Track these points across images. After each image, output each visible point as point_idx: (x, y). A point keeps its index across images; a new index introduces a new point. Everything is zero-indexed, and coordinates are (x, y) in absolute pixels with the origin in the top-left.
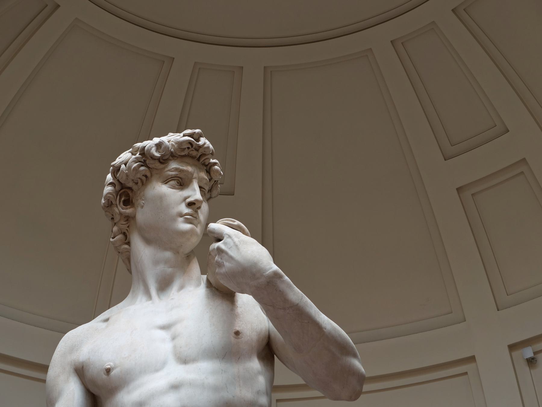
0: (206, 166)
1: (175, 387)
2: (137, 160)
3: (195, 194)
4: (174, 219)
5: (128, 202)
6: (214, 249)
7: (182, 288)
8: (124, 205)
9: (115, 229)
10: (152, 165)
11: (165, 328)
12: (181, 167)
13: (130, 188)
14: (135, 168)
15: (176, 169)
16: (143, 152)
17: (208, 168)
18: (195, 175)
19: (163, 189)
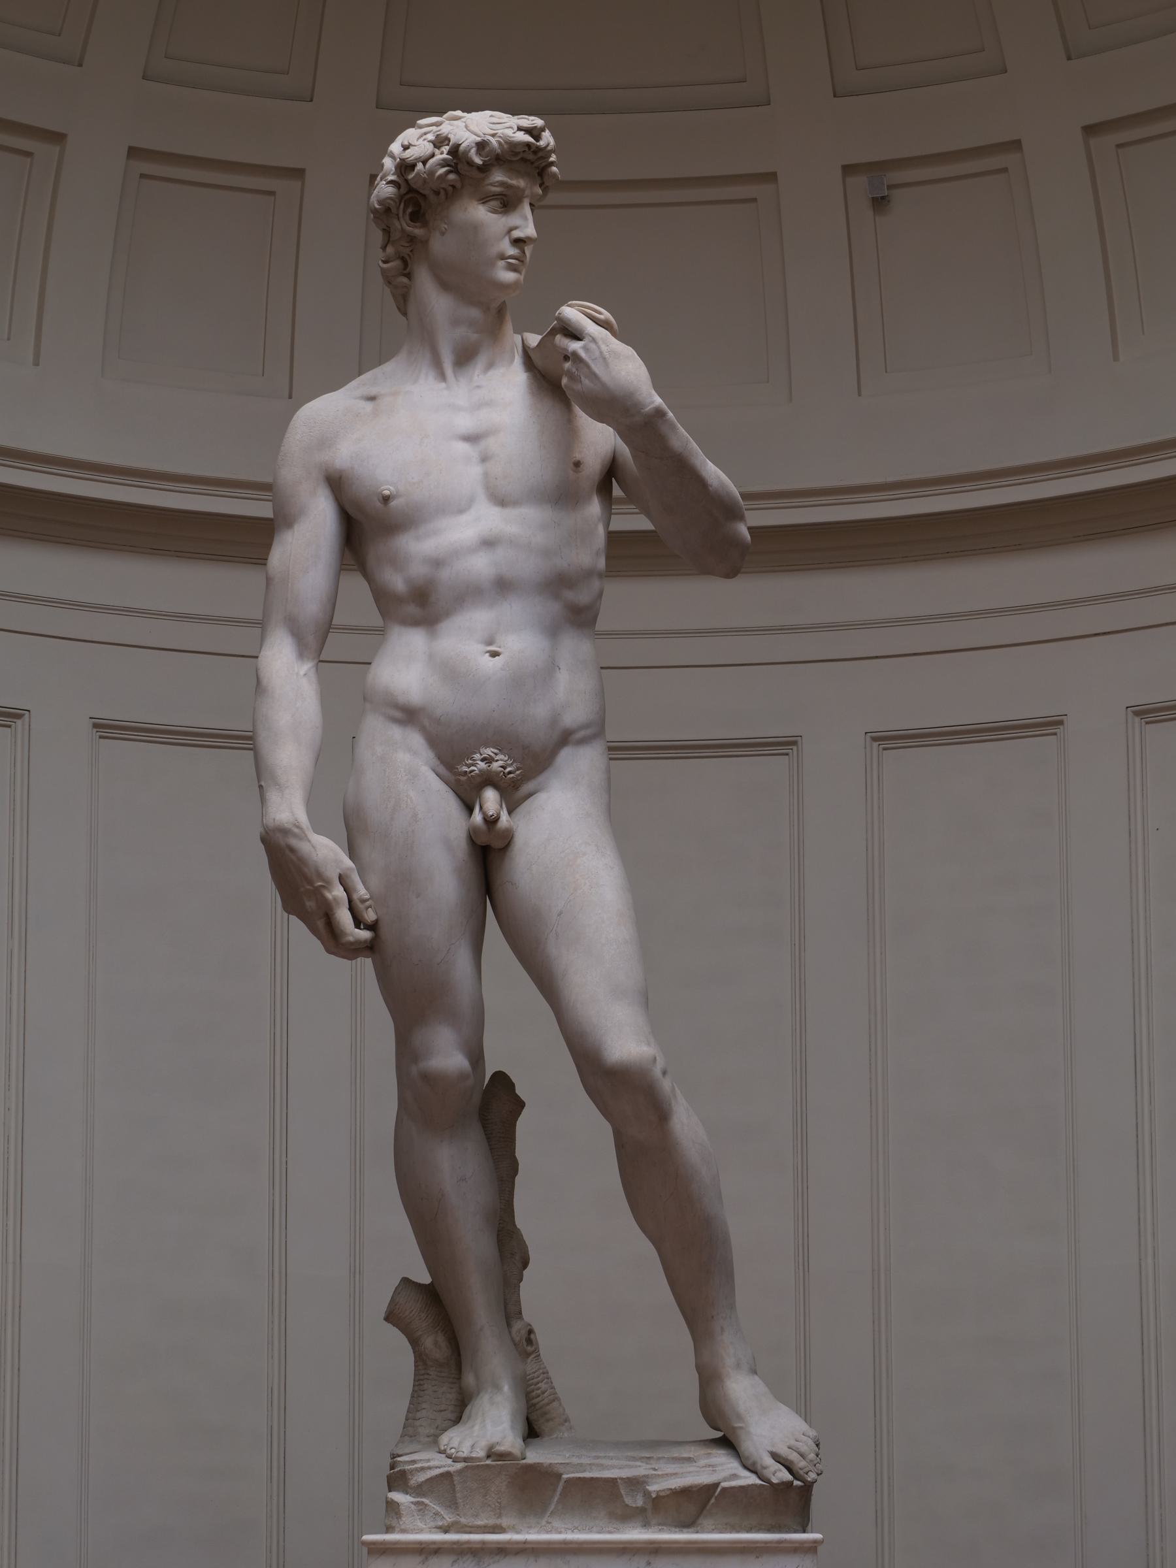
1: (489, 543)
2: (444, 163)
3: (527, 227)
4: (491, 264)
5: (417, 216)
6: (566, 350)
7: (490, 366)
8: (411, 220)
9: (390, 250)
10: (466, 170)
11: (472, 438)
12: (510, 181)
13: (424, 196)
14: (441, 175)
15: (502, 184)
16: (455, 151)
18: (527, 192)
19: (480, 213)
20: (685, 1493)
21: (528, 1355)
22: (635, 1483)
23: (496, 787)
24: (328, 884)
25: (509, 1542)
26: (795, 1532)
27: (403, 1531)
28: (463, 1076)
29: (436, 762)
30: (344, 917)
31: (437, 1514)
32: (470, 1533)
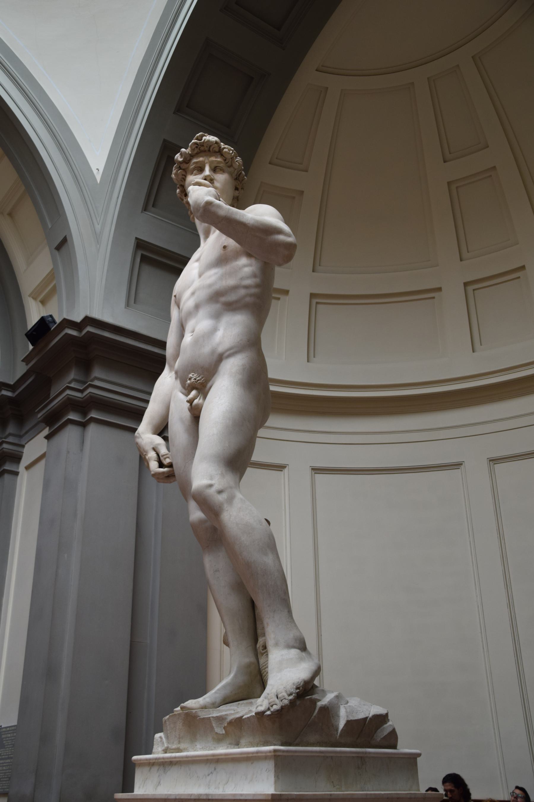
0: (217, 152)
1: (193, 294)
2: (176, 168)
17: (220, 152)
18: (206, 161)
20: (231, 723)
21: (262, 654)
22: (220, 719)
23: (196, 389)
24: (147, 452)
25: (171, 758)
26: (275, 745)
27: (154, 754)
28: (201, 522)
29: (182, 388)
30: (154, 466)
31: (163, 743)
32: (173, 753)
